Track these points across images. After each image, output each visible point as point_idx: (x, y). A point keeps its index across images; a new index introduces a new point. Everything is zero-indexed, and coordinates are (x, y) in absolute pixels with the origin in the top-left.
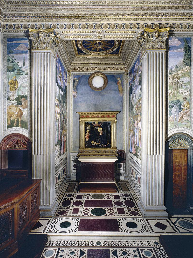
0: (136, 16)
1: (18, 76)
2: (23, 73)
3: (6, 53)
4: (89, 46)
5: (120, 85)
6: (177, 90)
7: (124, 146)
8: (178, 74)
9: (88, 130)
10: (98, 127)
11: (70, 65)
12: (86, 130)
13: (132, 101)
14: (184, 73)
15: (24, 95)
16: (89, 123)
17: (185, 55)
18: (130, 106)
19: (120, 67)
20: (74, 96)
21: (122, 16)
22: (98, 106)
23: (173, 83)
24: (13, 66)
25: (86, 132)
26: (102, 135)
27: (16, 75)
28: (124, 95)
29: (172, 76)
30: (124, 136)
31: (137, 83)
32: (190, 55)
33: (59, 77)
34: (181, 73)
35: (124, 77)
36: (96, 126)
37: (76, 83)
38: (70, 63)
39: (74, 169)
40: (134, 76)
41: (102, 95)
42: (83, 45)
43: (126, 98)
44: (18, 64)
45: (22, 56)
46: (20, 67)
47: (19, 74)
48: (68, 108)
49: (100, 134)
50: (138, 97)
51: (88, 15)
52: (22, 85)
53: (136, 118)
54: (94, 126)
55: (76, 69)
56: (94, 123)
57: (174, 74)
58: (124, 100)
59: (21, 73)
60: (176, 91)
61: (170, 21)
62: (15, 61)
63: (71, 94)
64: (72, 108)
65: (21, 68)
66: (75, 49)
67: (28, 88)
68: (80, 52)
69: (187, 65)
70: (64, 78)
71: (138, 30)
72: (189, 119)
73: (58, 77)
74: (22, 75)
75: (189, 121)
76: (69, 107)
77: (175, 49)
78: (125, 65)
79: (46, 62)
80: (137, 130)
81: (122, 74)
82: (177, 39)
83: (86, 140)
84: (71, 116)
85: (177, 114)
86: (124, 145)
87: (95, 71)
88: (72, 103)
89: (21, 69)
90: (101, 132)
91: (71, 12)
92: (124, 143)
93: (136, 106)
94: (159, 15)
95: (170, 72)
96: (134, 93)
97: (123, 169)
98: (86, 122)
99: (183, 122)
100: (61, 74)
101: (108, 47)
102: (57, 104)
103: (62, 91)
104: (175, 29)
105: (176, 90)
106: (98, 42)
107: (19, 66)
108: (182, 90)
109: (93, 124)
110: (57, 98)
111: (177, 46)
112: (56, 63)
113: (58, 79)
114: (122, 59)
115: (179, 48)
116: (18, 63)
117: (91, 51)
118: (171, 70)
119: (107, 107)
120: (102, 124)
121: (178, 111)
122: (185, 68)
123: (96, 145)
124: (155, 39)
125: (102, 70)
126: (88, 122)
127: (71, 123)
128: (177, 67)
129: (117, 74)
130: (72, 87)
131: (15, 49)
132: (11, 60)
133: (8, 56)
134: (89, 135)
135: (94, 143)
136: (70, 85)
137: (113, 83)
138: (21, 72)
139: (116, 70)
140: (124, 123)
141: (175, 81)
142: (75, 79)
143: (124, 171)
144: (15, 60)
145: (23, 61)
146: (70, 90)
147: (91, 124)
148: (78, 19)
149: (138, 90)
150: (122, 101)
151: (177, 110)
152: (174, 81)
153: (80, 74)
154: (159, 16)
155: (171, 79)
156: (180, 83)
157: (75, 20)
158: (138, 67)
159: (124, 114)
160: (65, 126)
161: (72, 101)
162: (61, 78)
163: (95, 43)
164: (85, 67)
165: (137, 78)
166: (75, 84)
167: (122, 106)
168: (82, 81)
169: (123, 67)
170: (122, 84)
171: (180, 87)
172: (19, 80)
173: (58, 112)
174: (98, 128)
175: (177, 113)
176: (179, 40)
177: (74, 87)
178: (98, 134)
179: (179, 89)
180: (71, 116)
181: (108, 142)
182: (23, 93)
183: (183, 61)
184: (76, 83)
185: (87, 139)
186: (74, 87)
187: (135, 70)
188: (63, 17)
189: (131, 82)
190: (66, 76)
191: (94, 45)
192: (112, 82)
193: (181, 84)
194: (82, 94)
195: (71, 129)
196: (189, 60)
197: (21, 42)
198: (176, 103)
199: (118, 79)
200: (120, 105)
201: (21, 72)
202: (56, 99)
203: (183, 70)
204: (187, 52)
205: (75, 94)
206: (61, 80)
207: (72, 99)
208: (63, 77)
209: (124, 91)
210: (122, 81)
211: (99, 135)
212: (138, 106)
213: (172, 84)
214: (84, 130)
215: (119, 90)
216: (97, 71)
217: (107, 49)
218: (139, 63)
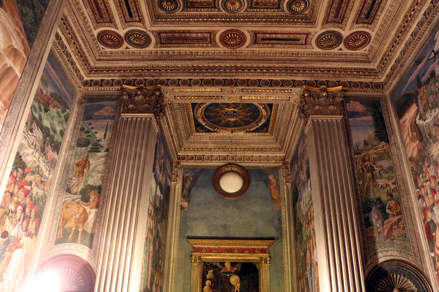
0: (289, 70)
1: (92, 153)
2: (100, 149)
3: (81, 118)
4: (216, 116)
5: (274, 188)
6: (374, 181)
8: (370, 155)
9: (209, 279)
10: (232, 273)
11: (179, 152)
12: (204, 279)
13: (299, 215)
14: (380, 153)
15: (96, 185)
16: (211, 265)
17: (376, 126)
18: (297, 228)
19: (274, 155)
20: (182, 208)
21: (268, 70)
22: (231, 230)
23: (365, 169)
24: (87, 138)
25: (203, 285)
26: (240, 291)
27: (89, 152)
28: (283, 207)
29: (361, 158)
31: (303, 177)
32: (384, 125)
33: (158, 164)
34: (375, 153)
35: (281, 173)
36: (226, 271)
37: (189, 183)
38: (181, 147)
40: (298, 167)
41: (239, 208)
42: (205, 115)
43: (287, 214)
44: (96, 135)
45: (105, 123)
46: (98, 139)
47: (94, 150)
48: (169, 231)
49: (235, 290)
50: (307, 202)
51: (216, 68)
52: (96, 169)
53: (308, 245)
54: (222, 271)
55: (190, 157)
56: (223, 264)
57: (363, 155)
58: (283, 218)
59: (98, 148)
60: (371, 183)
61: (342, 77)
62: (92, 130)
63: (177, 204)
64: (177, 232)
65: (100, 140)
66: (189, 121)
67: (104, 173)
68: (199, 128)
69: (383, 141)
70: (167, 170)
71: (293, 89)
72: (405, 234)
73: (157, 163)
74: (99, 151)
75: (406, 237)
76: (172, 229)
77: (359, 117)
78: (283, 152)
79: (141, 132)
80: (311, 270)
81: (277, 168)
82: (358, 103)
84: (175, 249)
85: (380, 223)
87: (225, 161)
88: (178, 221)
89: (100, 142)
90: (237, 285)
91: (190, 64)
93: (306, 222)
94: (324, 70)
95: (356, 150)
96: (300, 198)
98: (204, 262)
99: (394, 239)
100: (163, 161)
101: (248, 119)
102: (151, 212)
103: (162, 193)
104: (351, 88)
105: (371, 181)
106: (232, 111)
107: (96, 137)
108: (381, 181)
109: (219, 266)
110: (151, 200)
111: (360, 112)
112: (157, 139)
113: (157, 167)
114: (275, 141)
115: (365, 115)
116: (96, 133)
117: (219, 125)
118: (357, 147)
119: (248, 232)
120: (240, 267)
121: (380, 219)
122: (380, 146)
124: (322, 99)
125: (239, 160)
126: (208, 263)
127: (174, 264)
128: (366, 143)
129: (268, 168)
130: (180, 191)
131: (95, 114)
132: (86, 129)
133: (83, 123)
134: (211, 291)
136: (177, 186)
137: (262, 185)
138: (98, 147)
139: (266, 161)
140: (286, 266)
141: (367, 165)
142: (187, 175)
144: (92, 128)
145: (105, 130)
146: (176, 195)
147: (216, 267)
148: (200, 72)
149: (306, 189)
150: (280, 219)
151: (380, 216)
152: (365, 166)
153: (197, 166)
154: (324, 71)
155: (359, 163)
156: (375, 168)
157: (194, 74)
158: (302, 149)
159: (285, 247)
160: (160, 264)
161: (178, 218)
162: (162, 168)
163: (227, 112)
164: (207, 155)
165: (303, 168)
166: (187, 185)
167: (279, 229)
168: (200, 179)
169: (278, 155)
170: (278, 187)
171: (378, 175)
172: (91, 161)
173: (151, 228)
174: (230, 276)
175: (380, 222)
176: (361, 103)
177: (185, 191)
179: (376, 178)
180: (175, 249)
182: (96, 182)
183: (374, 134)
184: (189, 183)
186: (185, 191)
187: (299, 156)
188: (178, 70)
189: (295, 180)
190: (170, 168)
191: (225, 115)
192: (259, 182)
193: (378, 171)
194: (198, 204)
195: (173, 277)
196: (385, 133)
197: (107, 104)
198: (376, 203)
199: (271, 177)
200: (276, 228)
201: (98, 147)
202: (150, 200)
203: (377, 148)
204: (379, 120)
205: (186, 204)
206: (162, 172)
207: (179, 215)
208: (165, 168)
209: (283, 200)
210: (277, 180)
212: (309, 218)
213: (363, 171)
214: (199, 281)
215: (273, 199)
216: (230, 161)
217: (247, 123)
218: (304, 142)
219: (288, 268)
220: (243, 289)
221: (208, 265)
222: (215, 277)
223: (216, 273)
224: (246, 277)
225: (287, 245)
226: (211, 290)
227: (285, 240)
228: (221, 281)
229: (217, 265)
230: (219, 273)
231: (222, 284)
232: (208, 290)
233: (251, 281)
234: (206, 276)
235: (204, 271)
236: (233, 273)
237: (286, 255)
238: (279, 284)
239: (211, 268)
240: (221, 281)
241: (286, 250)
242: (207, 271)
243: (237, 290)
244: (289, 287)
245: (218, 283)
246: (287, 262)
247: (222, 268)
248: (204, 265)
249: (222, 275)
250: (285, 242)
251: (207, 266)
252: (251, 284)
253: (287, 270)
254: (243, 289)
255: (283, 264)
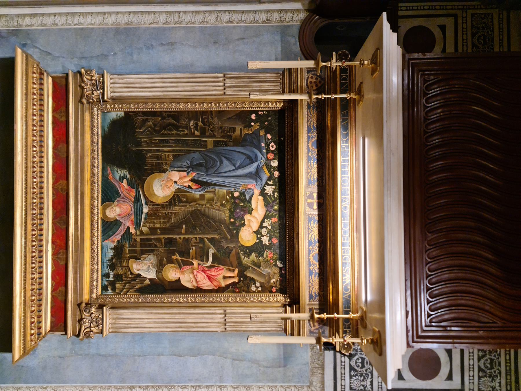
7: (276, 16)
10: (137, 199)
16: (112, 267)
26: (193, 170)
30: (201, 17)
36: (133, 217)
39: (450, 377)
54: (132, 230)
83: (233, 288)
86: (264, 17)
90: (176, 179)
92: (251, 17)
97: (441, 21)
98: (104, 288)
109: (117, 237)
120: (119, 173)
123: (266, 217)
126: (107, 275)
134: (195, 262)
135: (255, 226)
140: (111, 20)
143: (459, 12)
147: (118, 250)
159: (49, 21)
178: (191, 201)
181: (245, 132)
185: (225, 277)
211: (197, 194)
219: (118, 13)
220: (186, 162)
221: (114, 276)
222: (152, 251)
223: (138, 249)
224: (151, 151)
225: (43, 15)
226: (192, 264)
227: (28, 20)
228: (164, 231)
229: (112, 245)
230: (138, 239)
231: (175, 228)
232: (193, 273)
233: (163, 135)
234: (151, 280)
235: (132, 288)
236: (138, 192)
237: (76, 20)
238: (172, 44)
239: (122, 267)
240: (164, 231)
241: (61, 21)
242: (134, 279)
243: (192, 180)
244: (179, 12)
245: (170, 242)
246: (100, 18)
247: (121, 231)
248: (114, 289)
249: (145, 229)
250: (34, 21)
251: (118, 278)
252: (172, 135)
253: (123, 20)
254: (186, 162)
255: (105, 31)
